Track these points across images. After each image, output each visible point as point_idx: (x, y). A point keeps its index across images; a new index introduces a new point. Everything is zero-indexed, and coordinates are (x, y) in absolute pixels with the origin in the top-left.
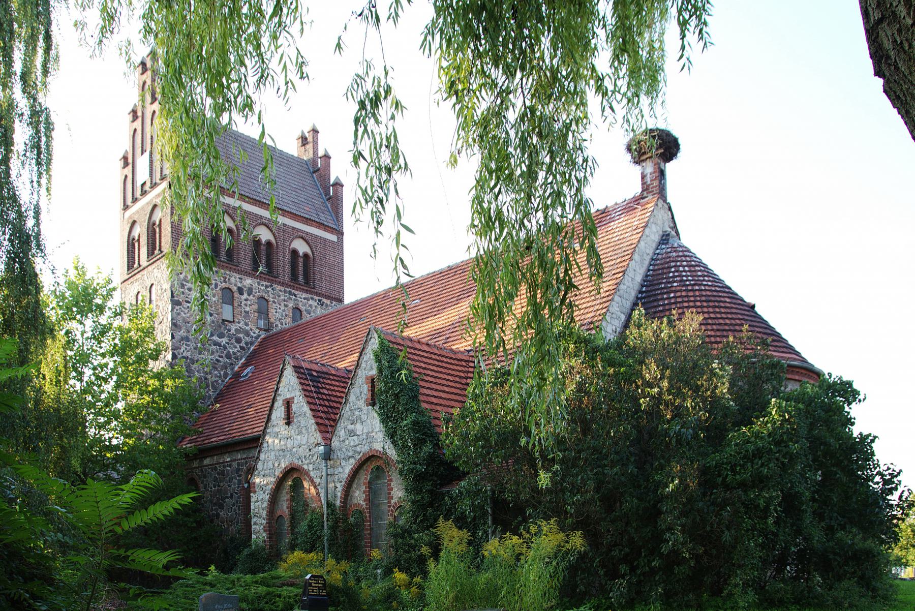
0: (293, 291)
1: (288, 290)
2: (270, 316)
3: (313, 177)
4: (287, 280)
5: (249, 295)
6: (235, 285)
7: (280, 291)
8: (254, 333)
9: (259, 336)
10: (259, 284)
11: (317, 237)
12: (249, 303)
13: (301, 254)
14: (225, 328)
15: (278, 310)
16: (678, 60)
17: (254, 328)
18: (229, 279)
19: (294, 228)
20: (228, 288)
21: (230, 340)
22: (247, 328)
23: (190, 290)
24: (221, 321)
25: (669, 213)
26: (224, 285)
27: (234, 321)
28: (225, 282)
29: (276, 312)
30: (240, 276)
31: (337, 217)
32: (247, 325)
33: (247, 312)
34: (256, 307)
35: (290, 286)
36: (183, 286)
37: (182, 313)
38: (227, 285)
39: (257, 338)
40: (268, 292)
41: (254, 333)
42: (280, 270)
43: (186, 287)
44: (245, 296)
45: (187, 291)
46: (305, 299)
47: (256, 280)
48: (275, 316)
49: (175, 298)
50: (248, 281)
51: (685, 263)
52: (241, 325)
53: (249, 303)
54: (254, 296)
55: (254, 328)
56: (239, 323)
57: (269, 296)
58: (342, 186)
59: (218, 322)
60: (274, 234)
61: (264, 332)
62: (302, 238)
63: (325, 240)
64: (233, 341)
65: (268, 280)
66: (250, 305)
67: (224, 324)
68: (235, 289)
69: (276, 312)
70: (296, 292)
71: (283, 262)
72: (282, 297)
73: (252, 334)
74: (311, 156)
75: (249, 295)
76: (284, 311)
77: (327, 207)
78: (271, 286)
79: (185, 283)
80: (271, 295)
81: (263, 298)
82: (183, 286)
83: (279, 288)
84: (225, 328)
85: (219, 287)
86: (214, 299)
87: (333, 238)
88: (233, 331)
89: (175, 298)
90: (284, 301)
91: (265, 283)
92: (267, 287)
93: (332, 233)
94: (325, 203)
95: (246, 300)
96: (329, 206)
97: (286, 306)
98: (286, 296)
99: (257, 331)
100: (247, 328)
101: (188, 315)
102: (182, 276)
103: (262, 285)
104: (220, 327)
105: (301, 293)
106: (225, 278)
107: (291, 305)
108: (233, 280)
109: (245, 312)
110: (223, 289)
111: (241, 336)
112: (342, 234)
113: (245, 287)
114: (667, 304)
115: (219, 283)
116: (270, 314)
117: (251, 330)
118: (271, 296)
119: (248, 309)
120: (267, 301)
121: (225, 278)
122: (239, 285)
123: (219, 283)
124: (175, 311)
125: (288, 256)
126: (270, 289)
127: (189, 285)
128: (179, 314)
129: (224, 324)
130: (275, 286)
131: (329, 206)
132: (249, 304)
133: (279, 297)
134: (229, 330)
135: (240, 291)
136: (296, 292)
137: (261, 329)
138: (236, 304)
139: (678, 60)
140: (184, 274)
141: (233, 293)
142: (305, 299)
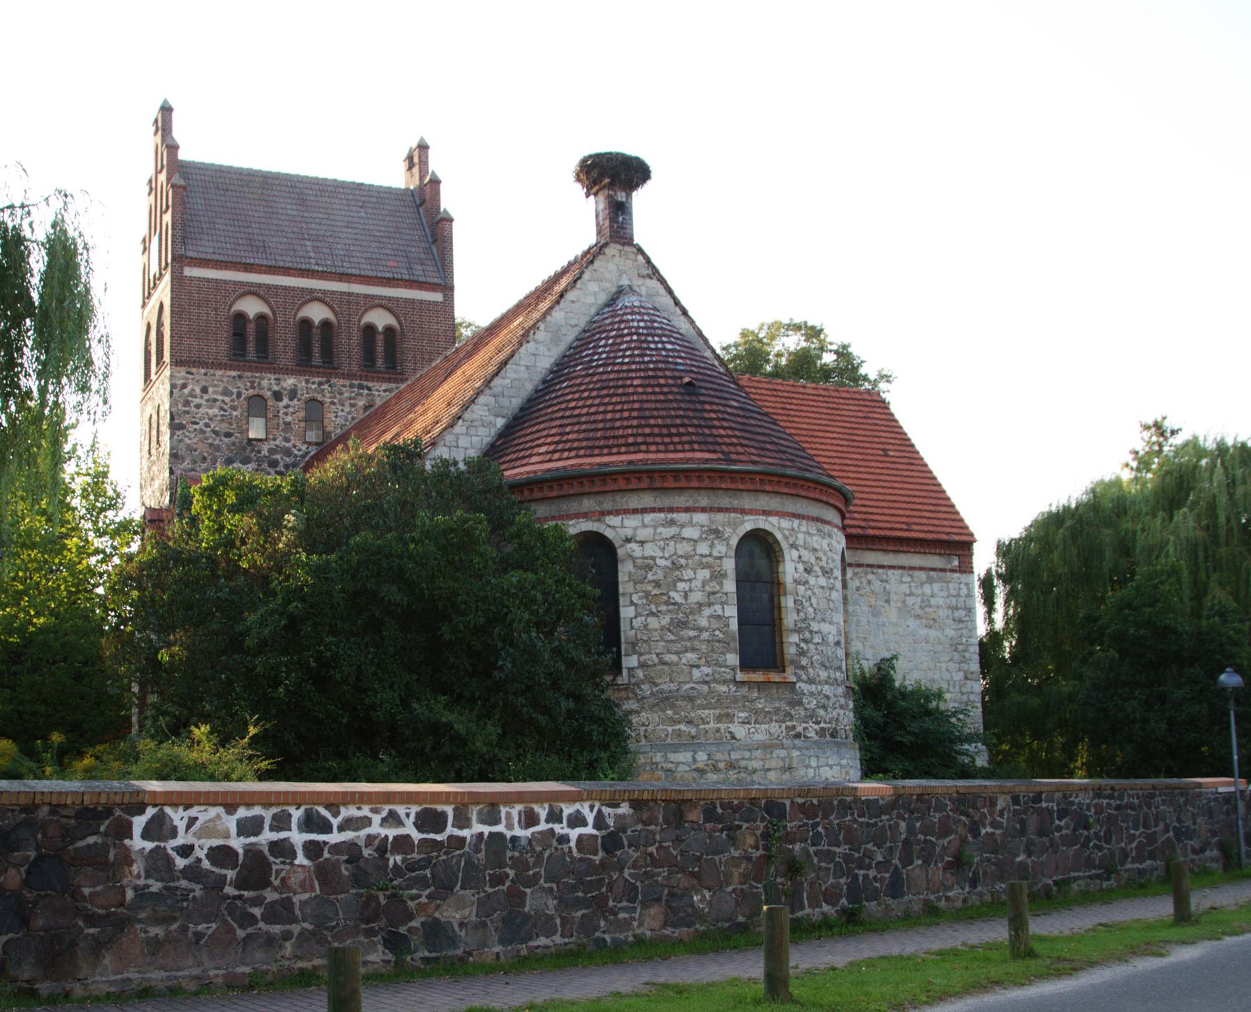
0: (365, 383)
1: (356, 382)
2: (325, 424)
3: (419, 212)
4: (355, 368)
5: (291, 400)
6: (269, 389)
7: (344, 386)
8: (300, 450)
9: (307, 453)
10: (307, 382)
11: (406, 300)
12: (291, 410)
13: (380, 328)
14: (253, 450)
15: (340, 414)
16: (166, 110)
17: (298, 444)
18: (259, 383)
19: (366, 296)
20: (258, 395)
21: (259, 465)
22: (287, 445)
23: (198, 406)
24: (245, 441)
25: (640, 257)
26: (251, 392)
27: (266, 439)
28: (253, 387)
29: (336, 417)
30: (277, 376)
31: (443, 265)
32: (287, 440)
33: (287, 424)
34: (302, 414)
35: (361, 377)
36: (187, 403)
37: (186, 440)
38: (256, 392)
39: (303, 457)
40: (323, 390)
41: (300, 450)
42: (344, 357)
43: (192, 404)
44: (285, 401)
45: (193, 409)
46: (385, 391)
47: (302, 378)
48: (334, 422)
49: (176, 421)
50: (290, 381)
51: (652, 346)
52: (277, 442)
53: (291, 410)
54: (299, 400)
55: (298, 444)
56: (275, 439)
57: (324, 396)
58: (451, 220)
59: (240, 443)
60: (332, 308)
61: (315, 447)
62: (381, 306)
63: (421, 302)
64: (265, 465)
65: (324, 374)
66: (293, 413)
67: (251, 445)
68: (268, 394)
69: (336, 417)
70: (370, 384)
71: (349, 347)
72: (346, 395)
73: (296, 452)
74: (417, 182)
75: (291, 400)
76: (350, 413)
77: (433, 254)
78: (328, 381)
79: (190, 399)
80: (328, 395)
81: (314, 400)
82: (187, 403)
83: (342, 382)
84: (253, 450)
85: (243, 396)
86: (235, 413)
87: (437, 297)
88: (265, 452)
89: (176, 421)
90: (350, 398)
91: (317, 380)
92: (320, 384)
93: (434, 290)
94: (430, 248)
95: (287, 407)
96: (434, 250)
97: (352, 406)
98: (351, 392)
99: (304, 448)
100: (287, 445)
101: (195, 440)
102: (186, 391)
103: (313, 383)
104: (245, 449)
105: (375, 384)
106: (253, 383)
107: (361, 403)
108: (265, 383)
109: (285, 423)
110: (249, 398)
111: (278, 457)
112: (451, 288)
113: (285, 389)
114: (610, 420)
115: (244, 391)
116: (326, 421)
117: (295, 446)
118: (328, 395)
119: (289, 419)
120: (322, 403)
121: (253, 383)
122: (276, 388)
123: (244, 391)
124: (176, 437)
125: (356, 338)
126: (326, 387)
127: (197, 401)
128: (181, 441)
129: (251, 445)
130: (333, 381)
131: (434, 250)
132: (290, 411)
133: (341, 394)
134: (259, 452)
135: (278, 396)
136: (370, 384)
137: (310, 444)
138: (270, 415)
139: (166, 110)
140: (190, 387)
141: (266, 400)
142: (385, 391)
